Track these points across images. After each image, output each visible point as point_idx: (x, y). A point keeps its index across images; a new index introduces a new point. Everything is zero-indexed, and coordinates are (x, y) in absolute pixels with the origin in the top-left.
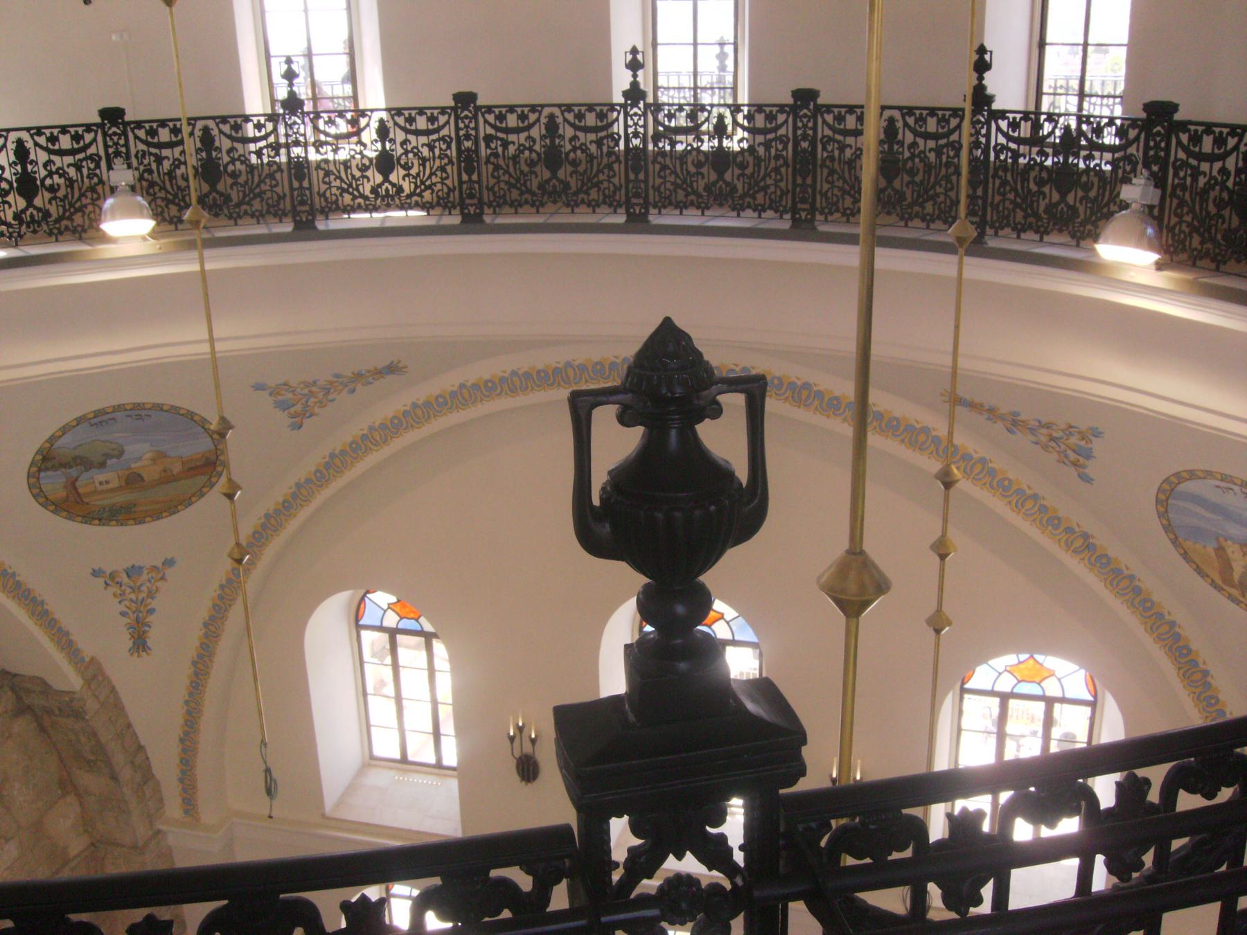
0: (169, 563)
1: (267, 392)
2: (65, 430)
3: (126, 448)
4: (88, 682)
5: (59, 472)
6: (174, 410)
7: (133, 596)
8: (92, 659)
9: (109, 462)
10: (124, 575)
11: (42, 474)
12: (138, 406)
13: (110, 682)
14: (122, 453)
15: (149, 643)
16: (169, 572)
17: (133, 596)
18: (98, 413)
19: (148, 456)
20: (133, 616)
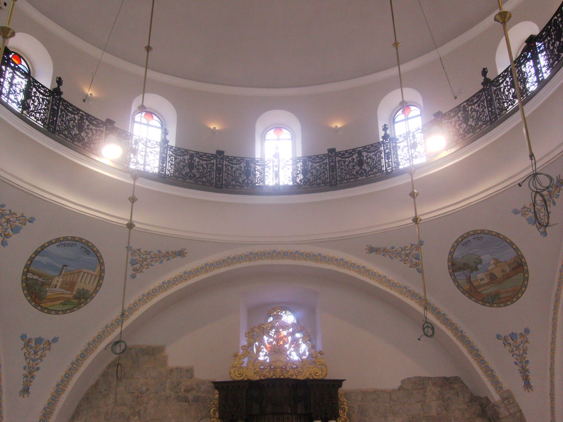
0: (527, 331)
1: (520, 214)
2: (454, 248)
3: (482, 258)
4: (504, 399)
5: (461, 273)
6: (490, 232)
7: (517, 352)
8: (508, 391)
9: (479, 266)
10: (510, 339)
11: (456, 274)
12: (475, 232)
13: (517, 406)
14: (481, 261)
15: (532, 383)
16: (528, 337)
17: (517, 352)
18: (463, 238)
19: (492, 262)
20: (520, 365)
